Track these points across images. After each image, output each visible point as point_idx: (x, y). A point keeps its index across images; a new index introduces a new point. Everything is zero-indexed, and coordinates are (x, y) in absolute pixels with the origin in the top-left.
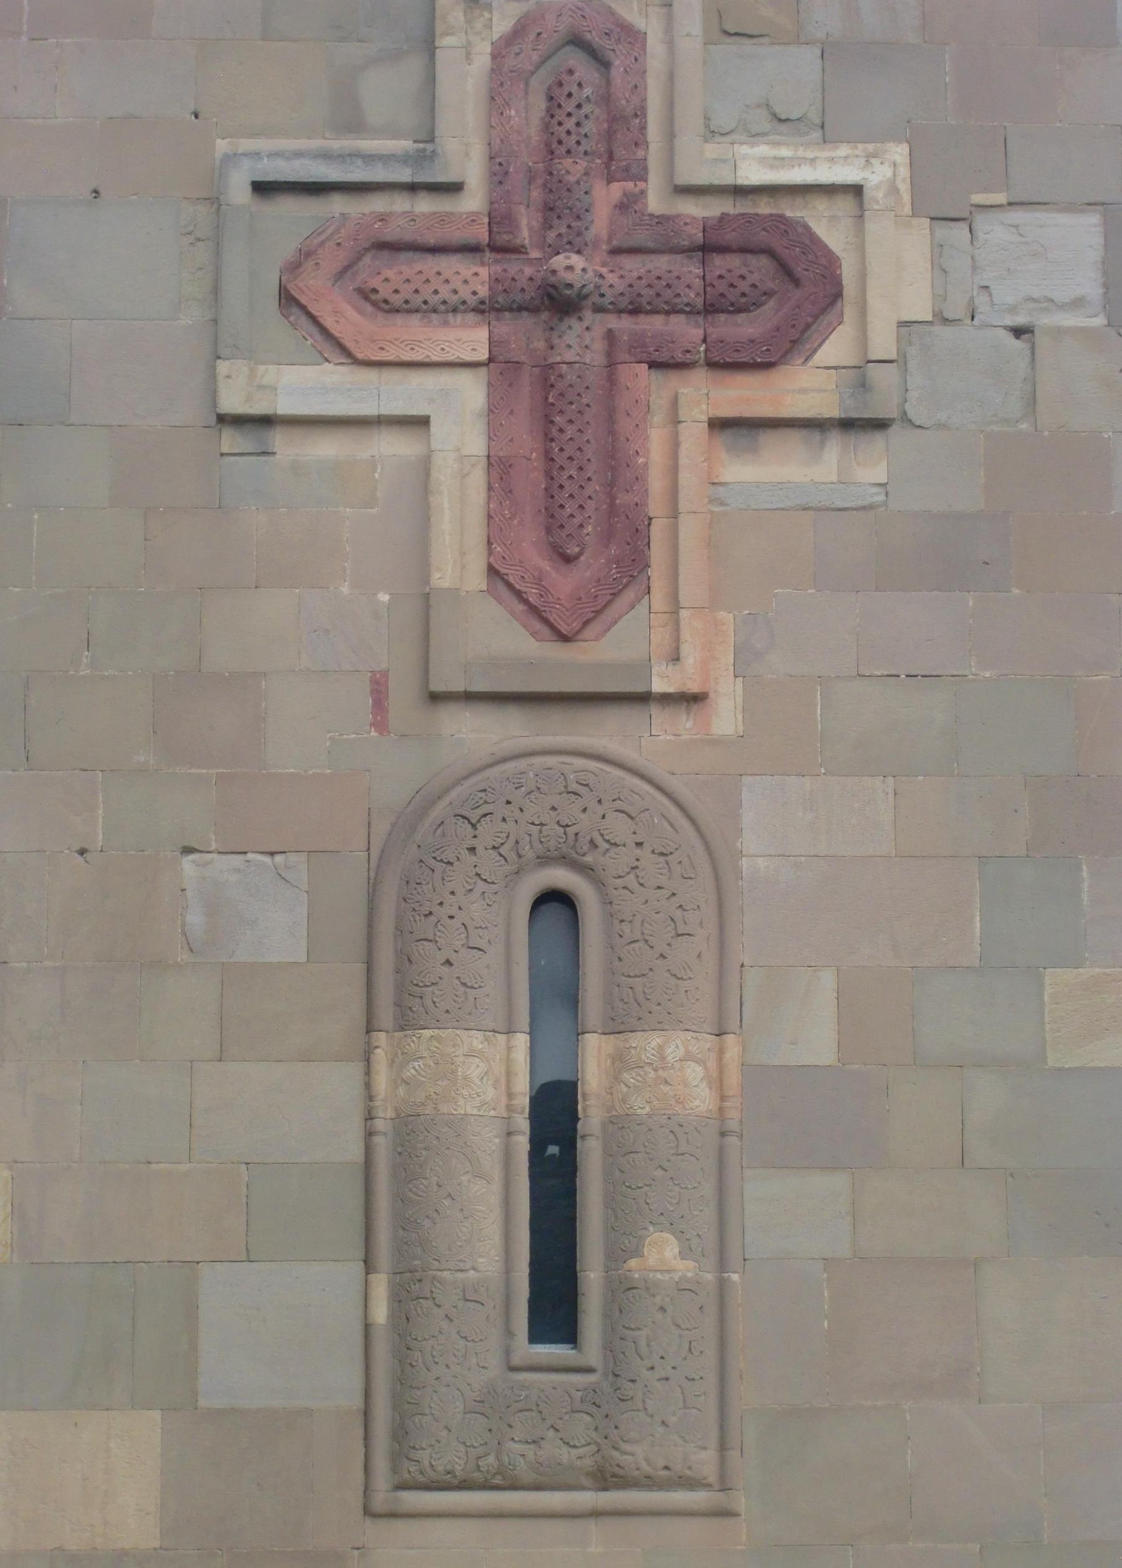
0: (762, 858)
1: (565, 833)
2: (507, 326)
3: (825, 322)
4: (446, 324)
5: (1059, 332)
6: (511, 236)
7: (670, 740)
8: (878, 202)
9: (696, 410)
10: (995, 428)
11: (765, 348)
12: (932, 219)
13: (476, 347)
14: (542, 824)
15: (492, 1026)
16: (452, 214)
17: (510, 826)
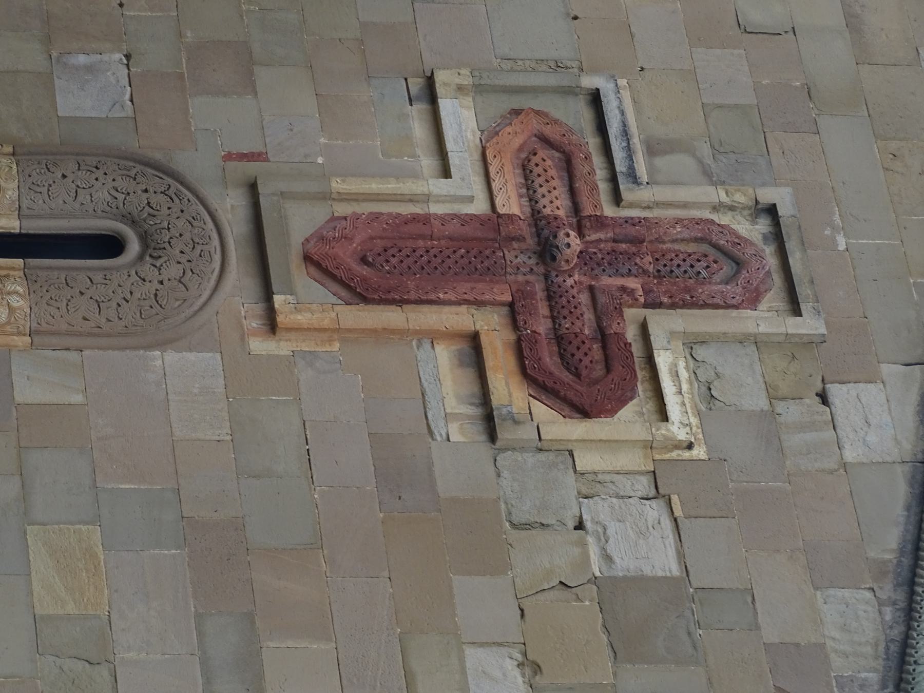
0: (161, 363)
1: (164, 242)
2: (526, 230)
3: (563, 407)
4: (521, 196)
5: (584, 545)
6: (589, 227)
7: (241, 313)
8: (658, 430)
9: (482, 323)
10: (503, 506)
11: (536, 366)
12: (654, 472)
13: (506, 207)
14: (169, 228)
15: (24, 206)
16: (599, 194)
17: (165, 211)
